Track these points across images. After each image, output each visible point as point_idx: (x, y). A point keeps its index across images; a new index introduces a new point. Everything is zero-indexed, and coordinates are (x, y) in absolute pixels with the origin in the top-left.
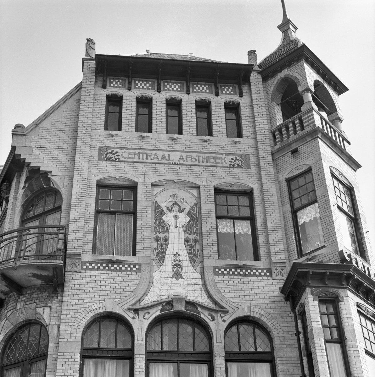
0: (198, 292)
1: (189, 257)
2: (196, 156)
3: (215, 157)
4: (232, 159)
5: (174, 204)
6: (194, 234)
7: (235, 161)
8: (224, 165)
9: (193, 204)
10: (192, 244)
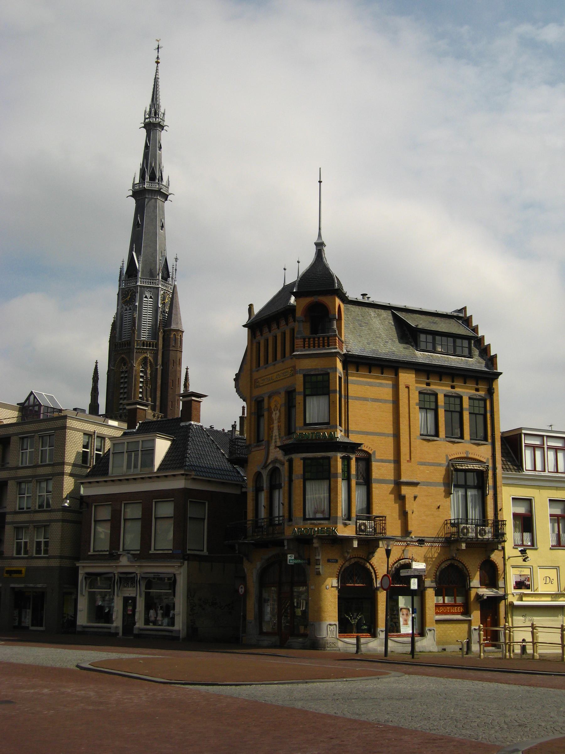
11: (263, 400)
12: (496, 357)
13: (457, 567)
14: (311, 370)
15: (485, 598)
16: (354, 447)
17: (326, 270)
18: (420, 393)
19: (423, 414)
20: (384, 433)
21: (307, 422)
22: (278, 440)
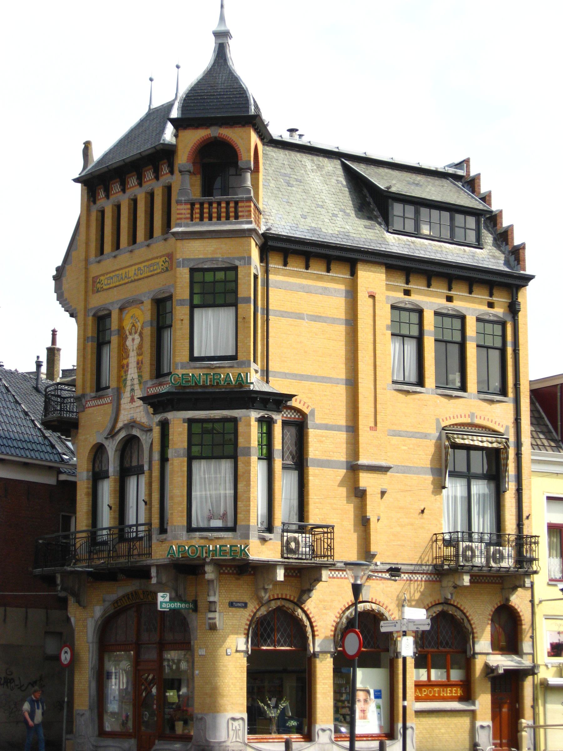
8: (159, 271)
11: (109, 315)
12: (524, 248)
13: (452, 617)
14: (205, 260)
15: (501, 671)
16: (279, 401)
17: (234, 79)
18: (393, 307)
19: (397, 345)
20: (330, 378)
21: (196, 354)
22: (137, 387)
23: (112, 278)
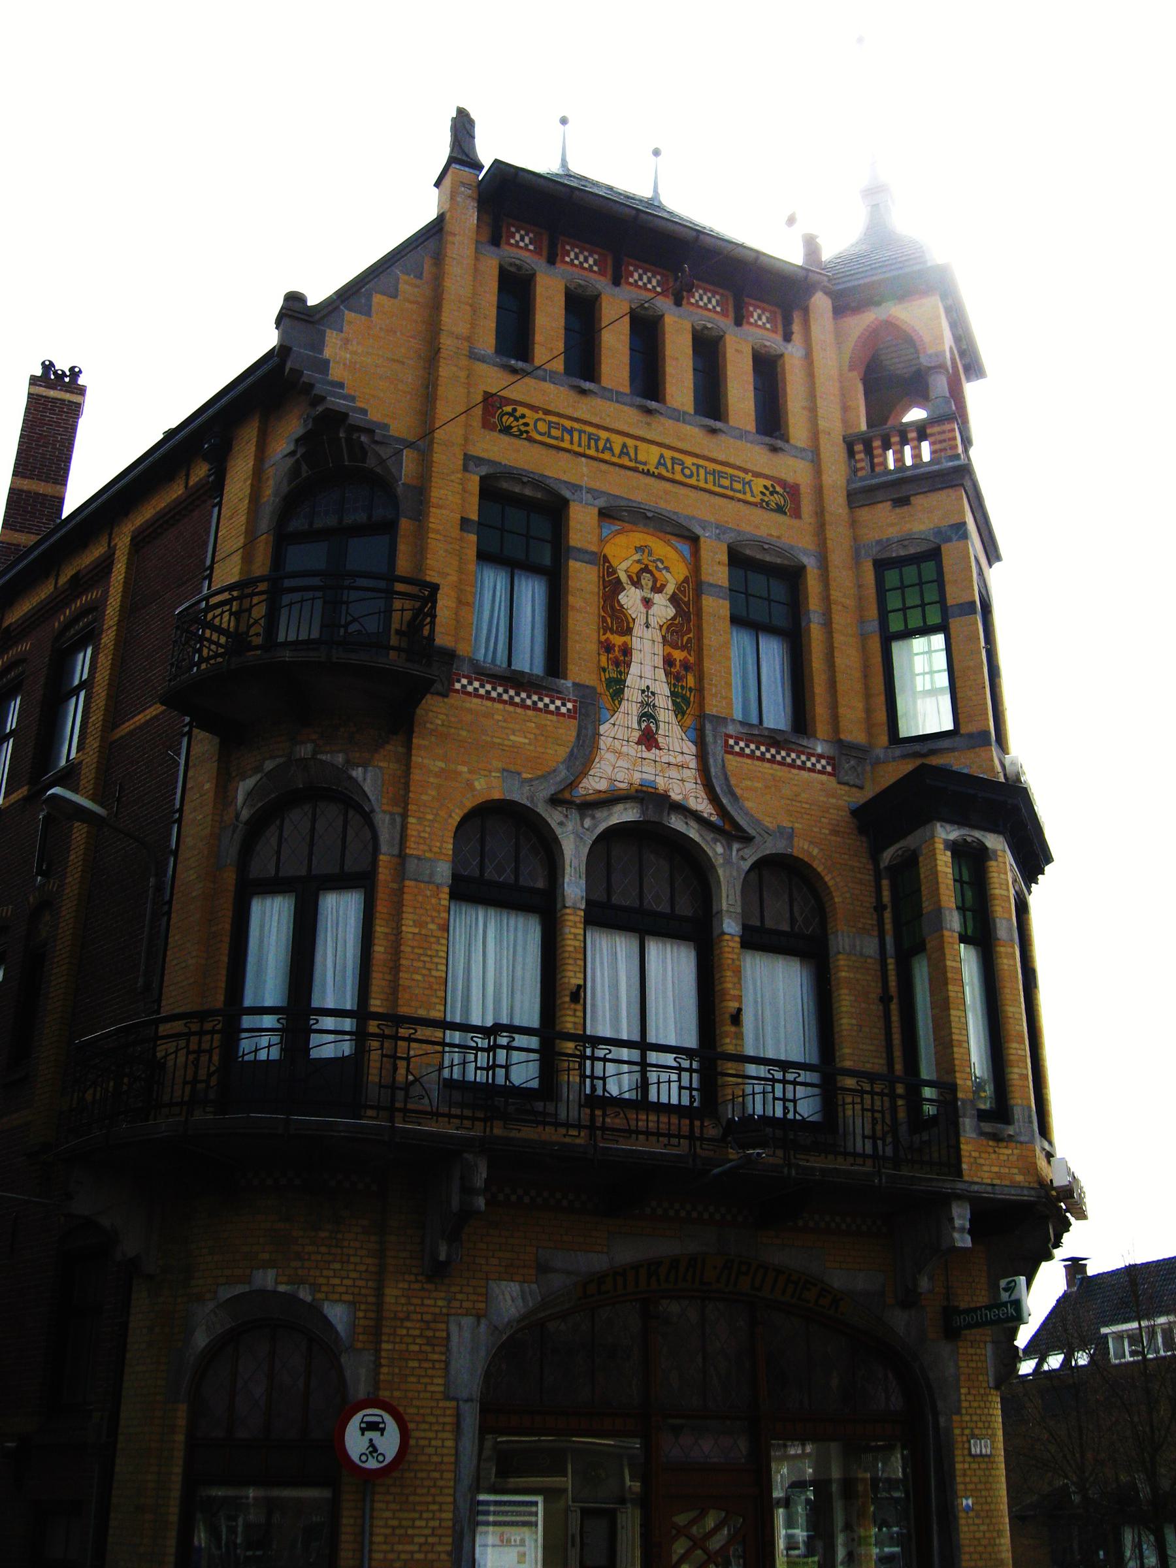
0: (690, 786)
1: (674, 703)
2: (693, 464)
3: (732, 476)
4: (766, 487)
5: (643, 570)
6: (683, 648)
7: (772, 494)
9: (682, 578)
10: (678, 673)
23: (570, 431)
